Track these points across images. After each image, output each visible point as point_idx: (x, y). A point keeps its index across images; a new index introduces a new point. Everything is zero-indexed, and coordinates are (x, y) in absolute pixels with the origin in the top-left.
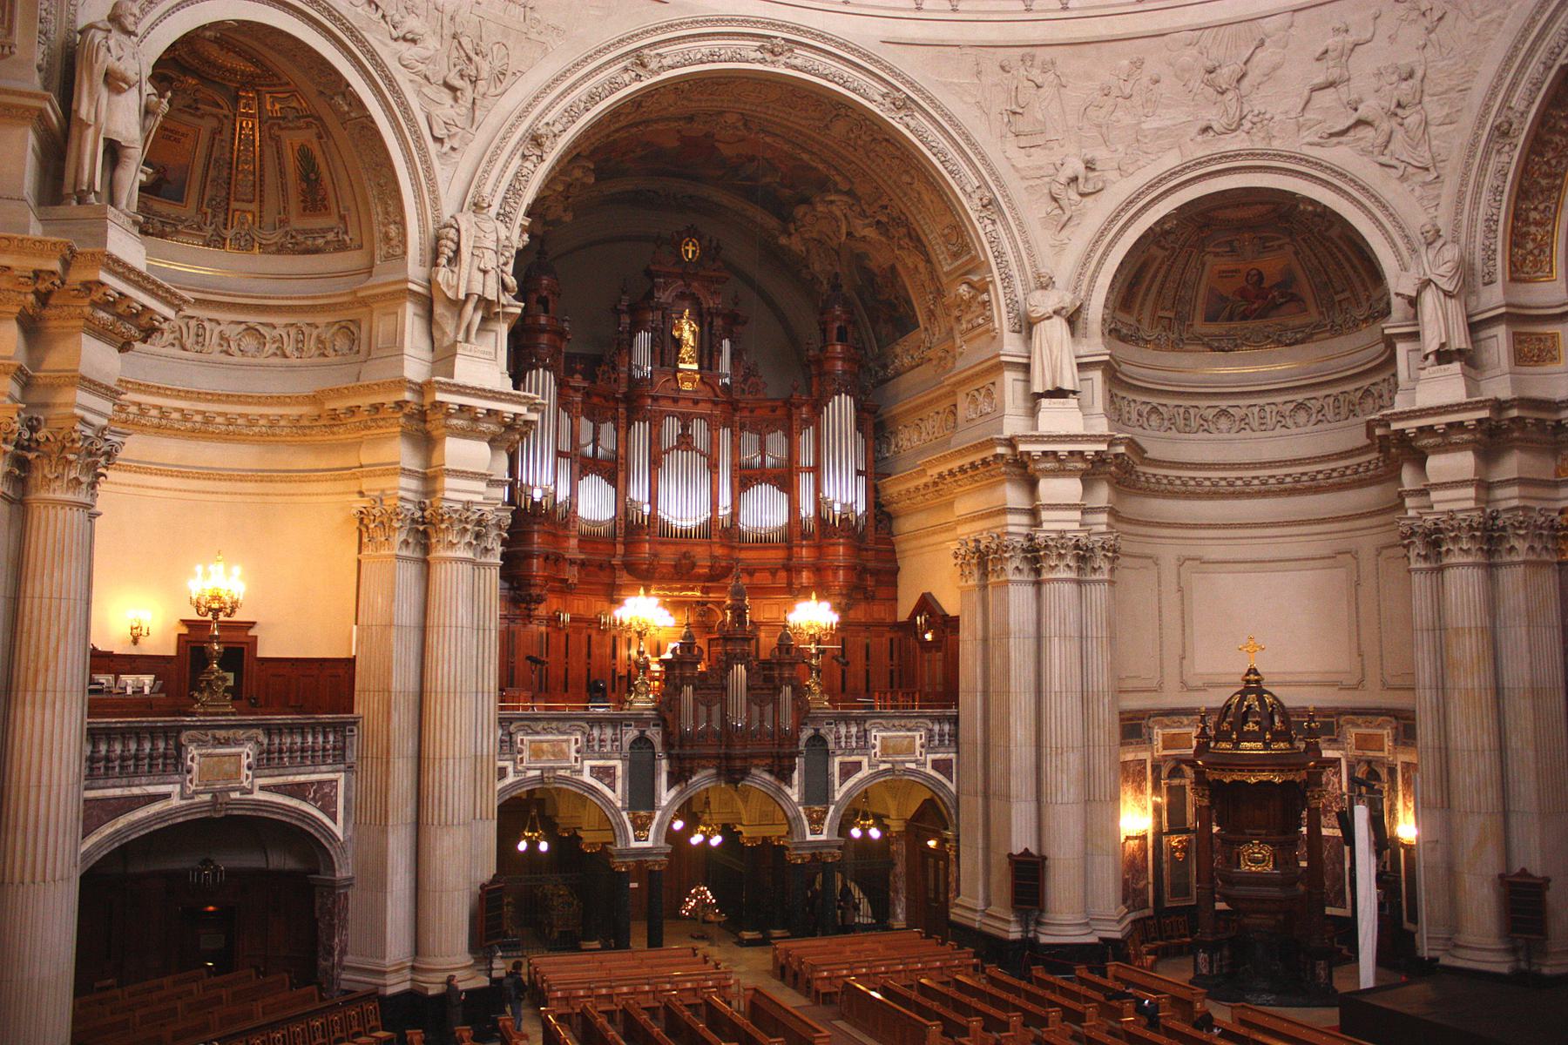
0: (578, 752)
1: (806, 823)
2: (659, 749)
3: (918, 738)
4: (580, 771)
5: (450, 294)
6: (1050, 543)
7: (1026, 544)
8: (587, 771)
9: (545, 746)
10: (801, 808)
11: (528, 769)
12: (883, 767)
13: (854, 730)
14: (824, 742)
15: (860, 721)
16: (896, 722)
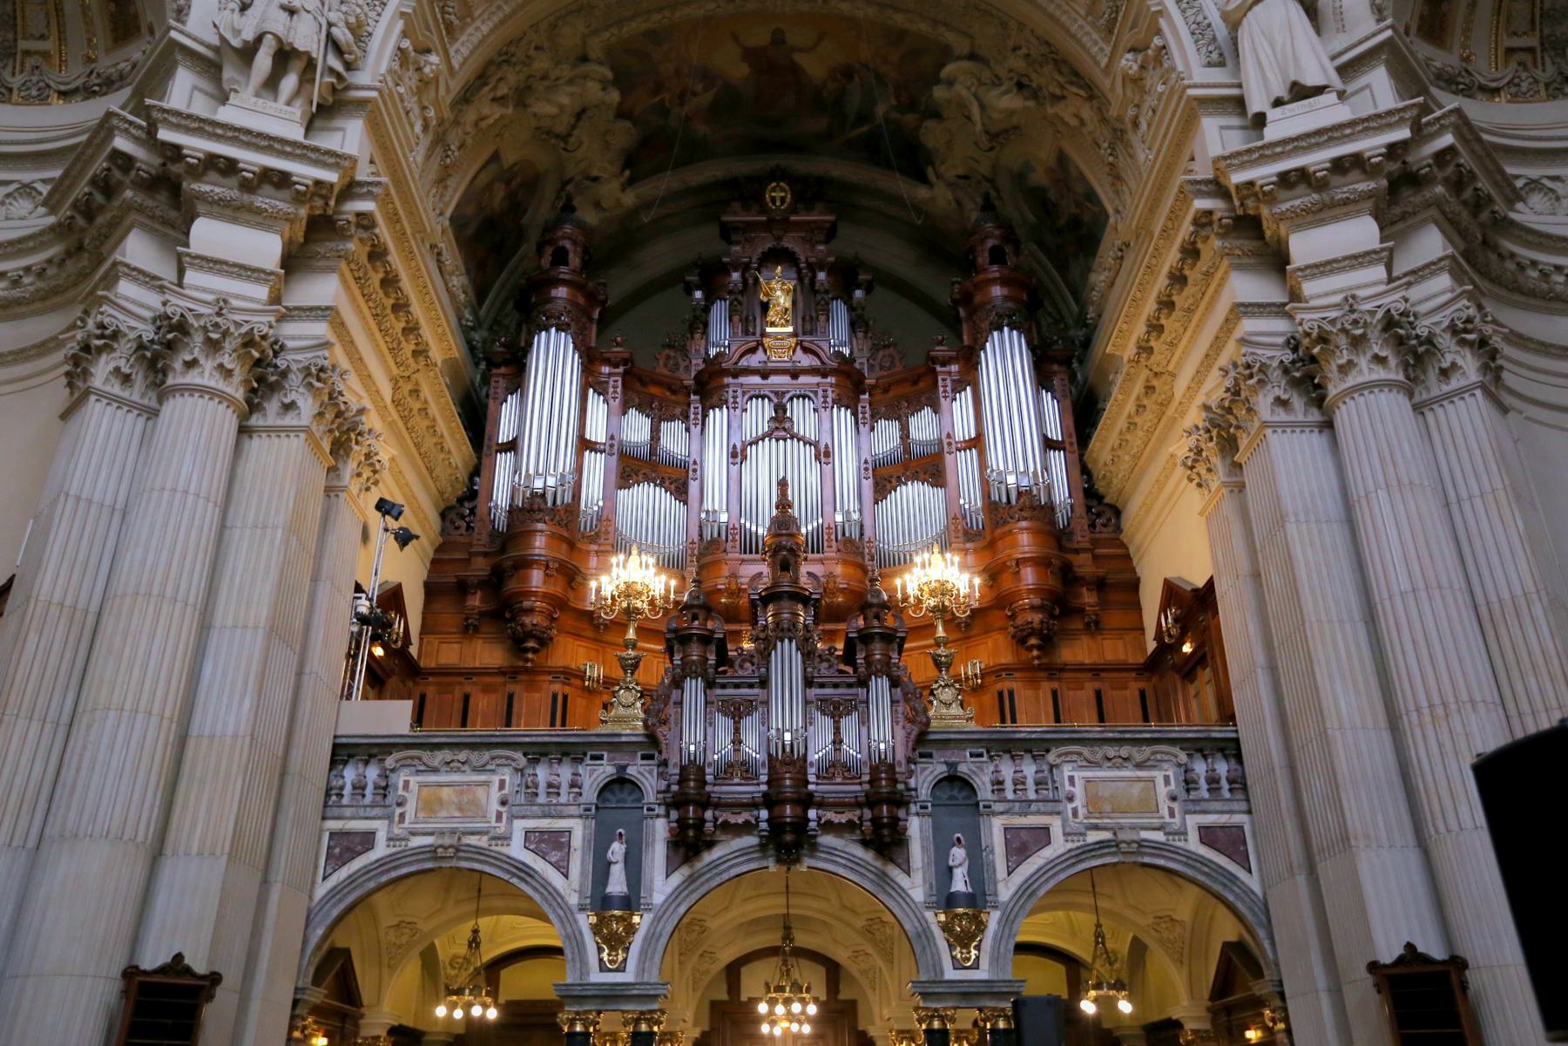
0: (503, 803)
1: (942, 945)
2: (650, 796)
3: (1160, 781)
4: (506, 838)
5: (236, 43)
6: (1328, 328)
7: (1288, 356)
8: (518, 838)
9: (446, 793)
10: (929, 915)
11: (413, 834)
12: (1093, 837)
13: (1029, 769)
14: (966, 785)
15: (1036, 748)
16: (1111, 751)
